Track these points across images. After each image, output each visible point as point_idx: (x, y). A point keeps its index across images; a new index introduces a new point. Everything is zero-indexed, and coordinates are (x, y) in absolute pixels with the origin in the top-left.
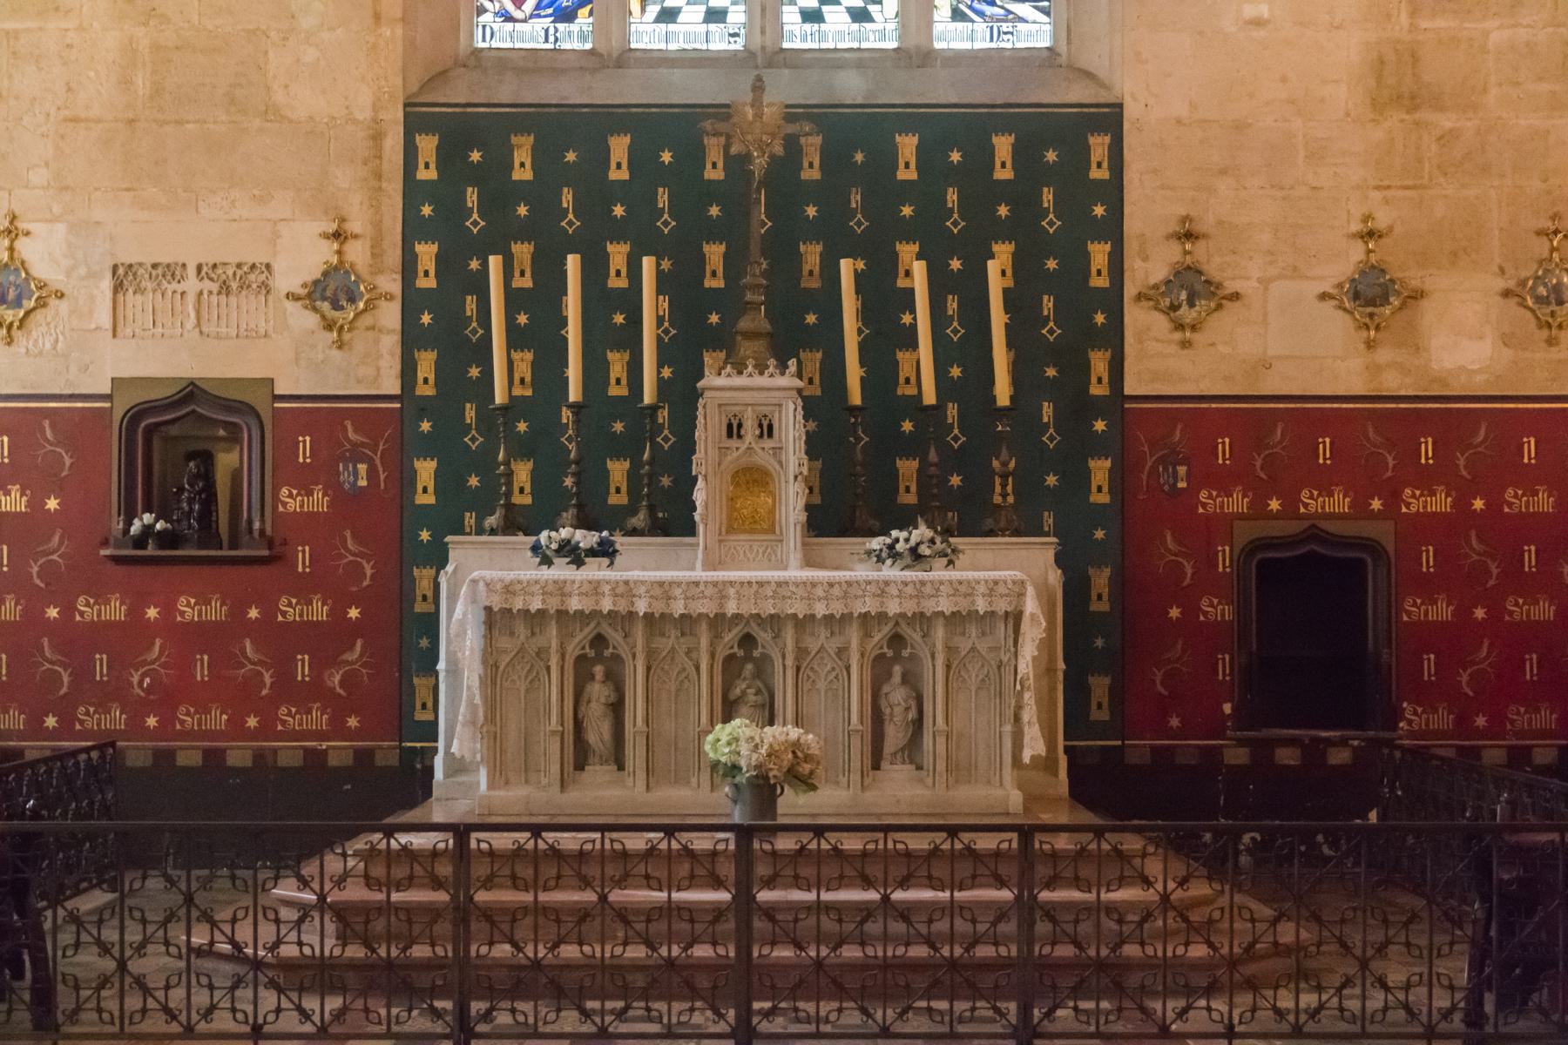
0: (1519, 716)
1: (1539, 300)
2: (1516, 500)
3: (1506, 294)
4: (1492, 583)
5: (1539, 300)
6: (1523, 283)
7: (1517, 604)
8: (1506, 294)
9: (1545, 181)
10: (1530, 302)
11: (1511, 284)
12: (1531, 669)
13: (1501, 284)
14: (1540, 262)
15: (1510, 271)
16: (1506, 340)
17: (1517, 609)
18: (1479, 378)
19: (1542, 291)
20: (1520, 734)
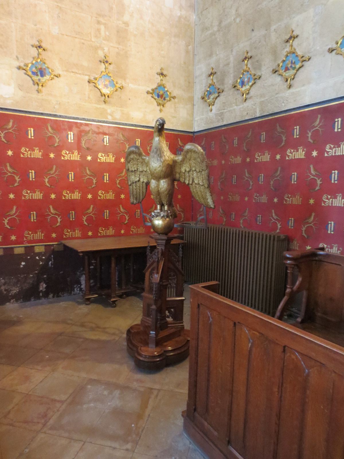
0: (29, 235)
1: (33, 73)
2: (25, 152)
3: (19, 68)
4: (16, 184)
5: (33, 73)
6: (26, 65)
7: (27, 193)
8: (19, 68)
9: (36, 25)
10: (30, 73)
11: (22, 65)
12: (33, 217)
13: (17, 64)
14: (34, 58)
15: (21, 59)
16: (20, 87)
17: (27, 195)
18: (9, 102)
19: (34, 69)
20: (29, 242)
